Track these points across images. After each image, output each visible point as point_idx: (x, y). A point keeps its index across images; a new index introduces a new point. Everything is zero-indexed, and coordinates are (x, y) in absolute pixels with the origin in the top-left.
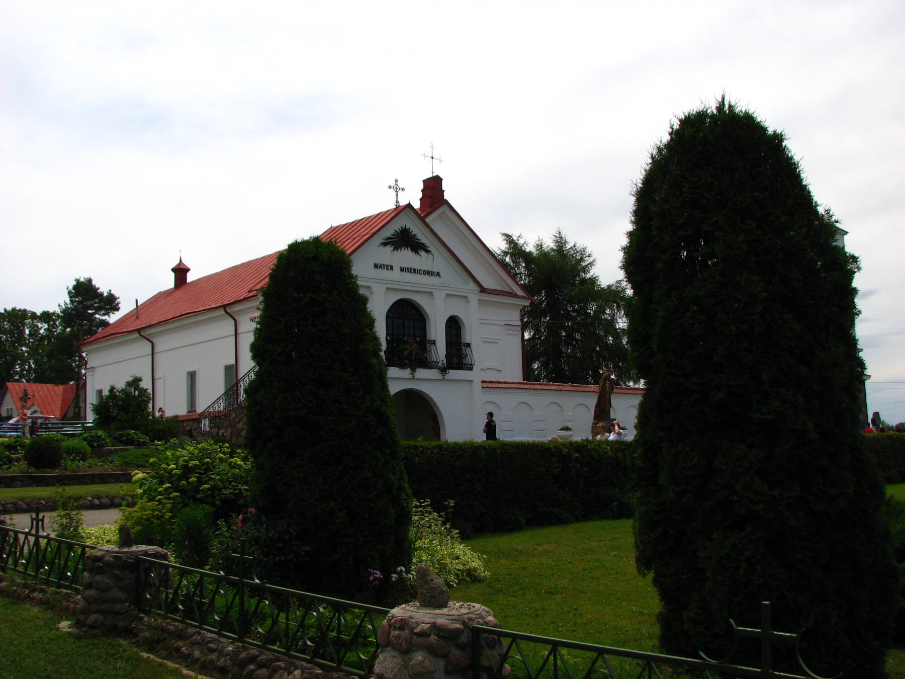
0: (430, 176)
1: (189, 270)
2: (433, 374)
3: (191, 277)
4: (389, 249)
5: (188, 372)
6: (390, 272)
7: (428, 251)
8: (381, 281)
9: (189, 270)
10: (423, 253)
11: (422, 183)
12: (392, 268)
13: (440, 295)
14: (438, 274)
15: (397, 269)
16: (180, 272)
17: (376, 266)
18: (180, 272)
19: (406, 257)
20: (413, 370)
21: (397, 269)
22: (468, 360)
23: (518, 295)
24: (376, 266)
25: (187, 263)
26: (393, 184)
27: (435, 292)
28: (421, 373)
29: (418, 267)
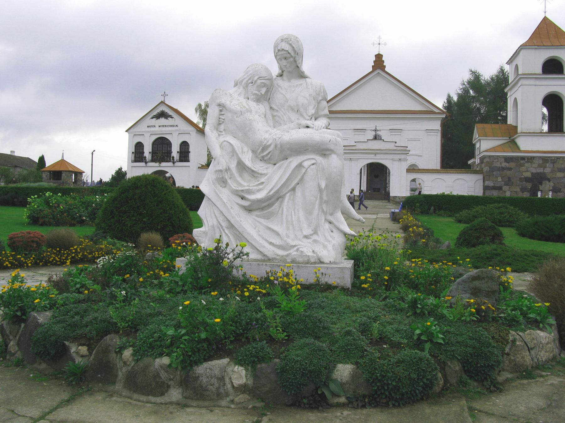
2: (170, 164)
4: (154, 119)
6: (154, 128)
7: (172, 118)
8: (148, 132)
10: (170, 119)
12: (155, 126)
13: (175, 134)
15: (157, 126)
17: (148, 127)
19: (162, 121)
20: (160, 163)
21: (157, 126)
24: (148, 127)
26: (166, 93)
27: (191, 133)
28: (163, 164)
29: (167, 124)
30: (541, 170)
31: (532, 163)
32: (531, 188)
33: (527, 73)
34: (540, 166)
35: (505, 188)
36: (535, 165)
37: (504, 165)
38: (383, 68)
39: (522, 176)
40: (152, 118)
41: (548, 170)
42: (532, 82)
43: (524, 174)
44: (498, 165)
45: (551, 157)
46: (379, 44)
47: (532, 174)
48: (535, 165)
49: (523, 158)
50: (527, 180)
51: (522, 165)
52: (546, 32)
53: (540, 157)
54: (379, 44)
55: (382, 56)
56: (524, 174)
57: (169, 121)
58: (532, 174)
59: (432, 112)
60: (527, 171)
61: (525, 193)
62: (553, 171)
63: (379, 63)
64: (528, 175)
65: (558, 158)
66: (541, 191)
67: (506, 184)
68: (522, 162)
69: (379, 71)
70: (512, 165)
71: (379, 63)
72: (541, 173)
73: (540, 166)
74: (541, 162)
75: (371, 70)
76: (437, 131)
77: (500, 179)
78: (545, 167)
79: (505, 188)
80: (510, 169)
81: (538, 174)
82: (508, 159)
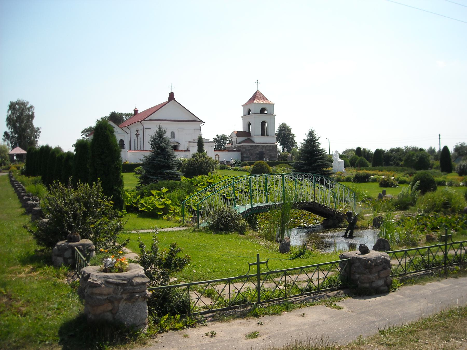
3: (139, 112)
14: (118, 132)
16: (136, 111)
18: (136, 111)
22: (125, 148)
25: (138, 109)
30: (262, 150)
34: (261, 148)
35: (251, 157)
37: (250, 148)
41: (264, 150)
44: (247, 148)
47: (259, 151)
49: (256, 146)
50: (257, 154)
51: (256, 148)
53: (262, 145)
60: (257, 150)
63: (171, 97)
64: (257, 152)
67: (251, 156)
68: (256, 147)
69: (173, 101)
70: (252, 148)
71: (171, 97)
75: (167, 100)
77: (249, 154)
78: (263, 149)
79: (251, 157)
80: (252, 150)
81: (261, 151)
82: (251, 146)
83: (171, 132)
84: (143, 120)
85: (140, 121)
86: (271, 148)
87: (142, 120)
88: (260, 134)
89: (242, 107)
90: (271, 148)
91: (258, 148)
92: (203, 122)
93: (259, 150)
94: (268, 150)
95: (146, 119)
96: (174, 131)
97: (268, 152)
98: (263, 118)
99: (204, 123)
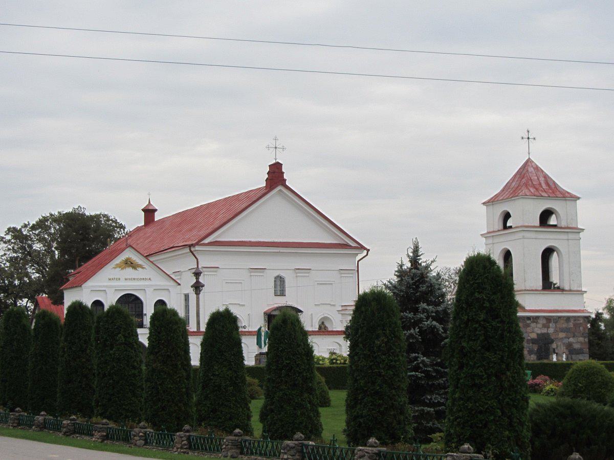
0: (274, 162)
1: (156, 210)
3: (158, 217)
4: (118, 269)
5: (192, 287)
7: (143, 268)
9: (156, 210)
10: (140, 269)
11: (268, 168)
12: (119, 279)
13: (149, 291)
16: (149, 213)
17: (109, 279)
18: (149, 213)
19: (129, 272)
23: (351, 246)
24: (109, 279)
30: (544, 331)
31: (537, 323)
32: (537, 350)
33: (527, 224)
34: (544, 326)
36: (540, 326)
38: (283, 182)
39: (529, 338)
40: (115, 268)
41: (551, 331)
42: (533, 235)
43: (530, 335)
45: (553, 316)
46: (276, 148)
47: (538, 334)
48: (540, 326)
49: (529, 318)
51: (528, 326)
52: (536, 178)
54: (276, 148)
55: (281, 165)
56: (530, 335)
57: (139, 273)
58: (538, 334)
59: (345, 246)
60: (533, 332)
61: (532, 356)
62: (556, 331)
63: (276, 175)
64: (534, 336)
65: (560, 317)
66: (557, 353)
68: (528, 322)
69: (280, 188)
71: (276, 175)
72: (545, 333)
73: (544, 326)
74: (545, 321)
76: (352, 272)
78: (548, 327)
81: (543, 334)
83: (275, 278)
84: (197, 244)
85: (190, 246)
86: (571, 325)
87: (194, 242)
88: (539, 284)
89: (485, 207)
90: (571, 325)
91: (533, 325)
92: (365, 249)
93: (539, 332)
94: (562, 330)
95: (207, 241)
96: (282, 274)
97: (562, 335)
98: (547, 239)
99: (368, 250)
